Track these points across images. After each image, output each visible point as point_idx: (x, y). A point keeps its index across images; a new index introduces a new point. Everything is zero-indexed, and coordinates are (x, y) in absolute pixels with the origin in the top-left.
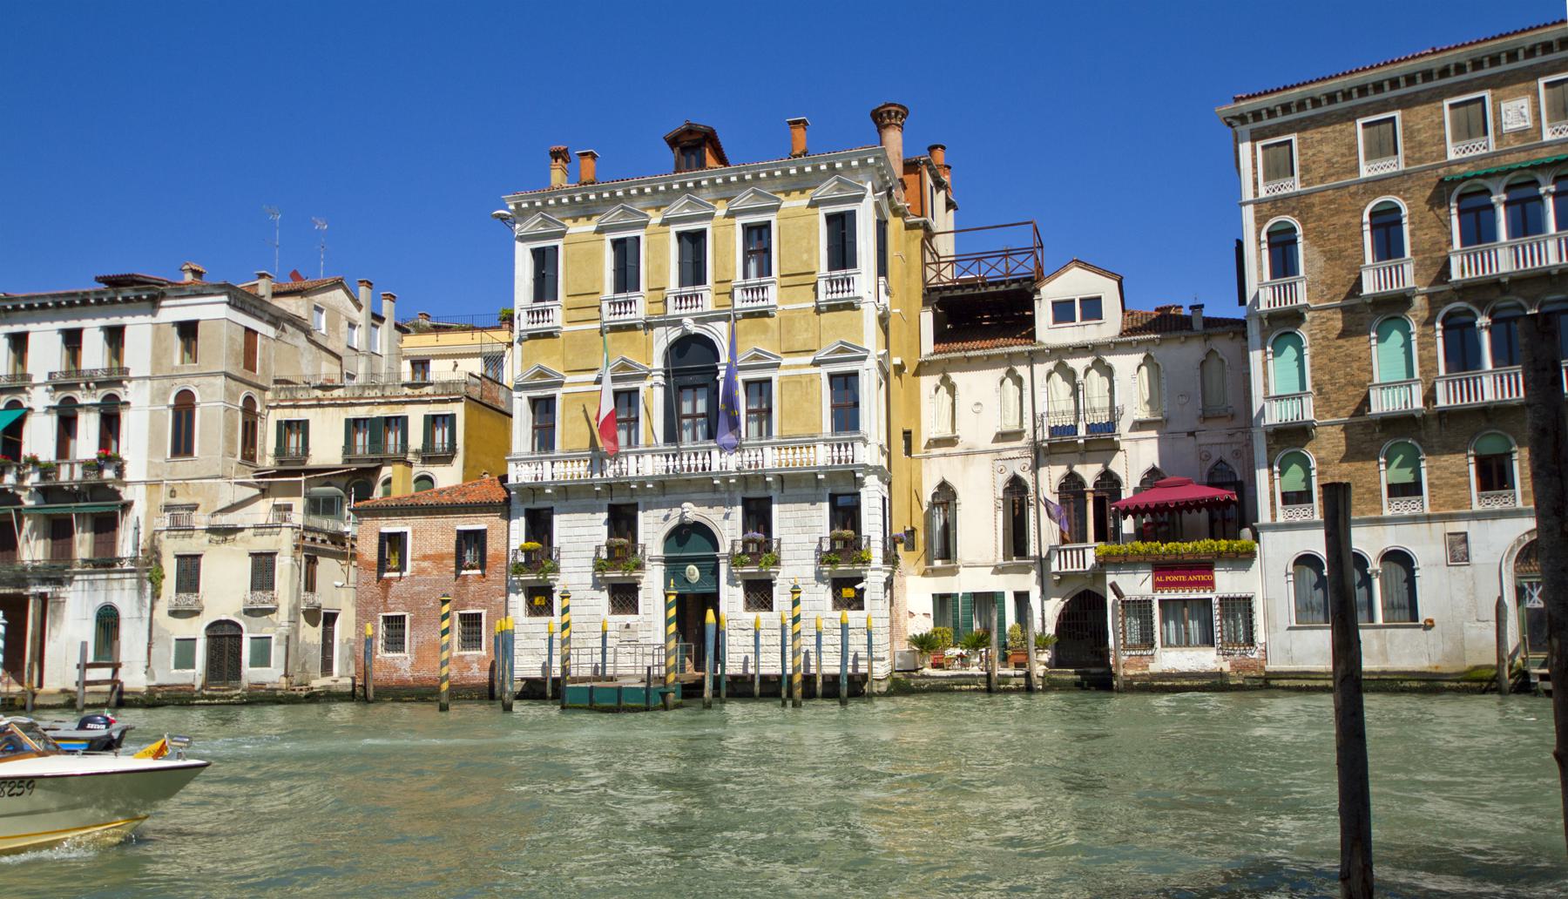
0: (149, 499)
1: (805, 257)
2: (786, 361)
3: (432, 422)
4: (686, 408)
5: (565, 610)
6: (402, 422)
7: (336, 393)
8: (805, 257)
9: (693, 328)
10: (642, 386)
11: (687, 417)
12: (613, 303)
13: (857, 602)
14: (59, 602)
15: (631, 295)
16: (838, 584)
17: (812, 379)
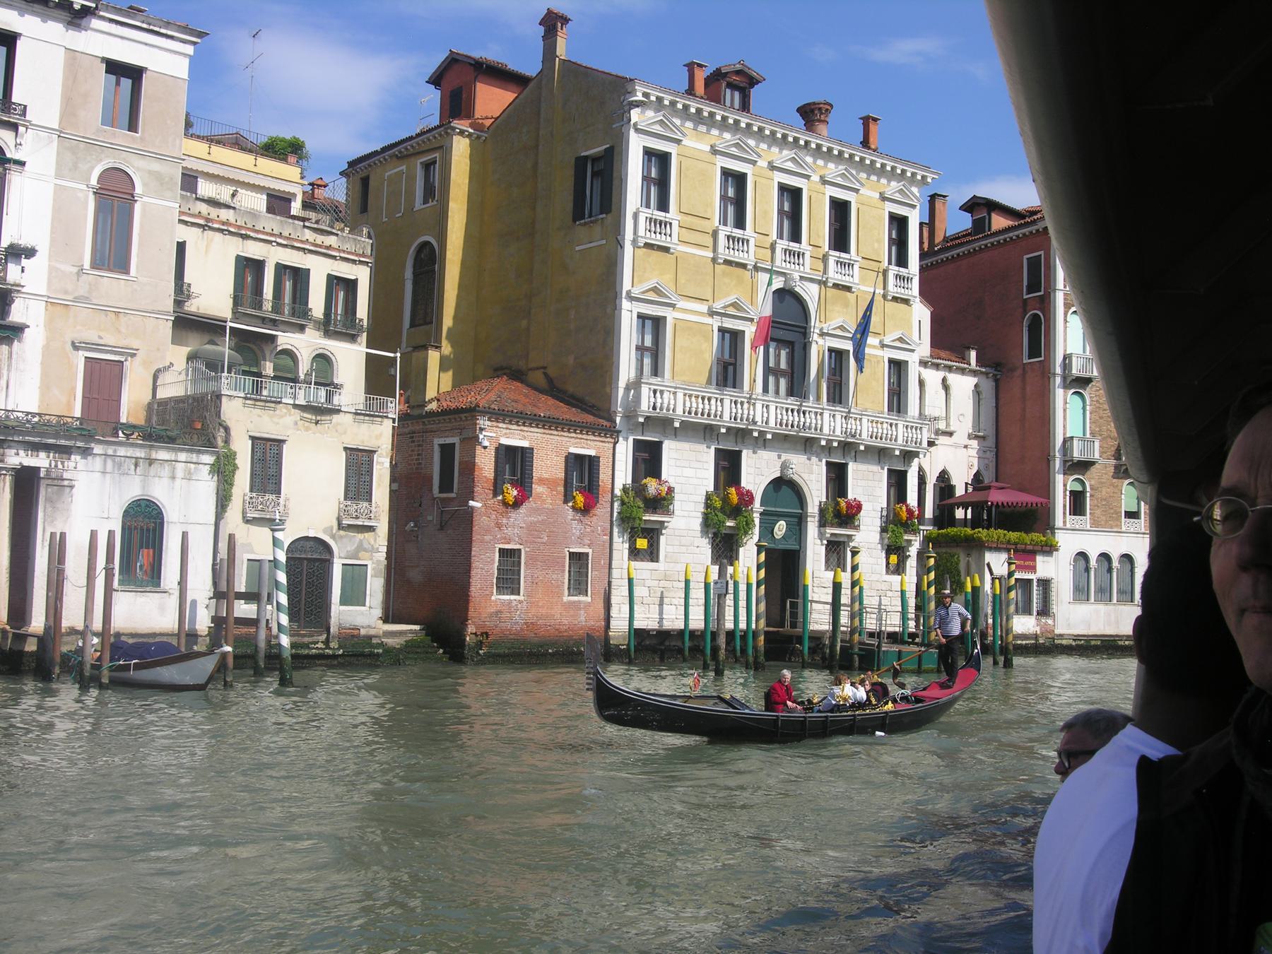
0: (50, 324)
5: (854, 568)
7: (225, 214)
14: (61, 484)
16: (890, 550)
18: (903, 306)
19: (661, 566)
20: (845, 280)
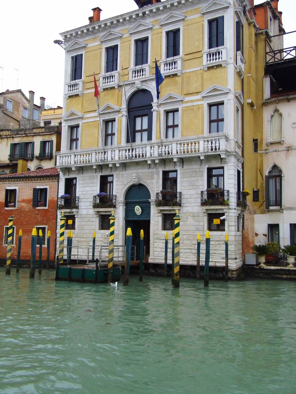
1: (197, 44)
2: (187, 99)
3: (44, 144)
4: (138, 127)
6: (33, 143)
8: (197, 44)
9: (139, 85)
10: (117, 117)
11: (139, 131)
12: (104, 78)
13: (221, 227)
15: (113, 73)
16: (211, 217)
17: (200, 107)
18: (219, 70)
19: (76, 231)
20: (173, 71)
